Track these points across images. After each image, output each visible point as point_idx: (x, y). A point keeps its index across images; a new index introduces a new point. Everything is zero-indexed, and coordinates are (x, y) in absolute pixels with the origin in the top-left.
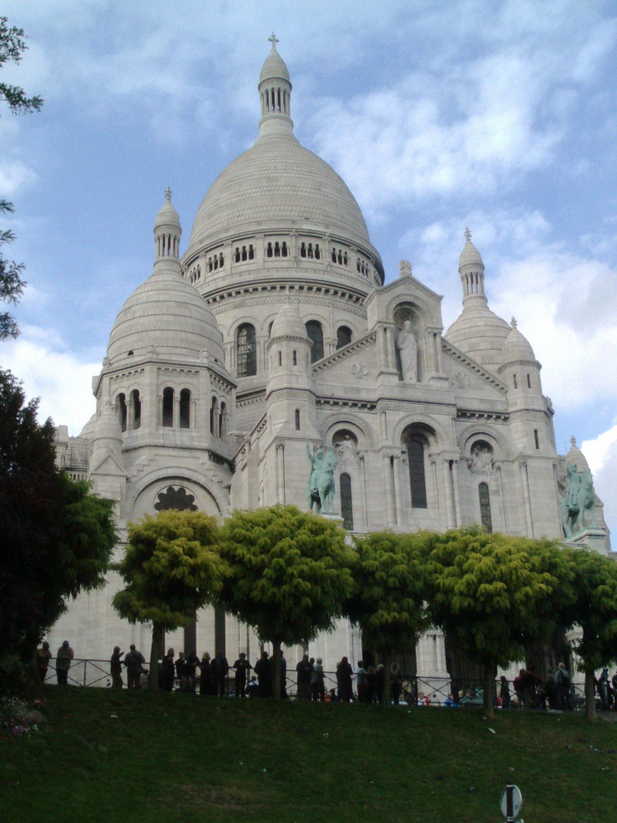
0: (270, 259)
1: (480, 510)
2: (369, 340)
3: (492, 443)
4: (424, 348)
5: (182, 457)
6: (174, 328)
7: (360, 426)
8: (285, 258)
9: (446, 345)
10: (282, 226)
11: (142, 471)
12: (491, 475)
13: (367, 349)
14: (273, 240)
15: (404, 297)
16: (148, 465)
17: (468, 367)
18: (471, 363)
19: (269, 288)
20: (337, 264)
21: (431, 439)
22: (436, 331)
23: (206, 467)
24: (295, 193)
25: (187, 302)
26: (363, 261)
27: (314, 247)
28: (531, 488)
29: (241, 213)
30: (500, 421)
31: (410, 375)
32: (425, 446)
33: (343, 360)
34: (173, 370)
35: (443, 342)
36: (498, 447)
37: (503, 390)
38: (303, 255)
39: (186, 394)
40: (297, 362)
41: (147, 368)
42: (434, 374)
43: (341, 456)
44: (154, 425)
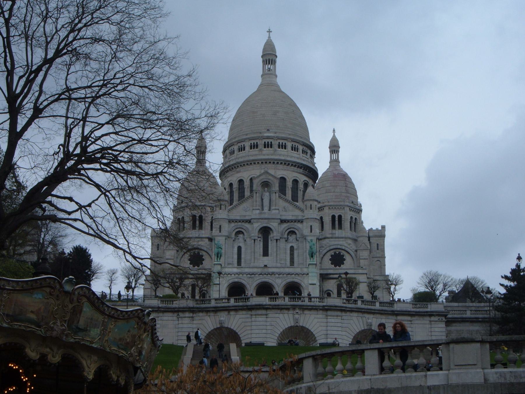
0: (251, 150)
3: (296, 231)
8: (257, 150)
10: (256, 135)
13: (250, 200)
14: (252, 142)
19: (249, 164)
20: (281, 149)
21: (271, 232)
23: (208, 244)
26: (295, 145)
27: (270, 143)
30: (299, 223)
31: (266, 209)
37: (302, 211)
38: (265, 147)
42: (274, 208)
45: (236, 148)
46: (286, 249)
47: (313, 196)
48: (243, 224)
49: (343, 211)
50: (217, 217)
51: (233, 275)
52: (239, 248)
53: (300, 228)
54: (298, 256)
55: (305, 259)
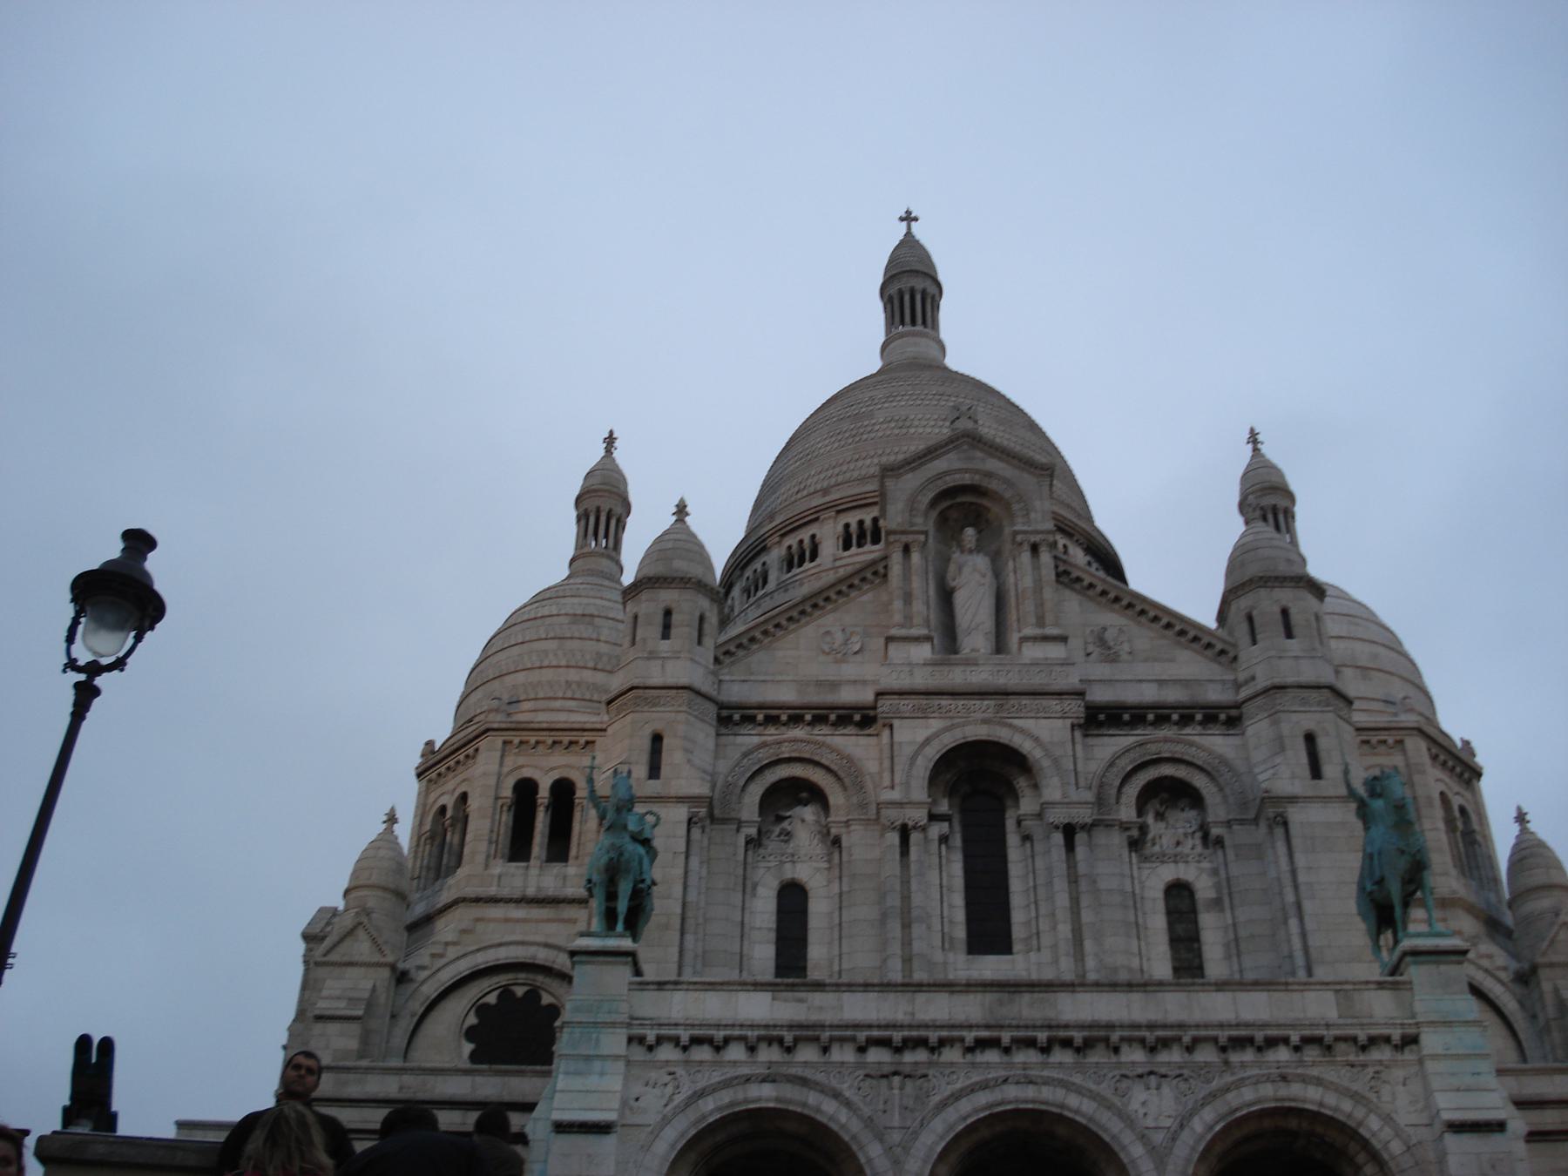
0: (847, 553)
1: (1168, 955)
2: (869, 575)
3: (1199, 781)
4: (1011, 579)
5: (538, 921)
6: (554, 663)
7: (833, 767)
9: (1069, 569)
11: (441, 956)
12: (1199, 862)
13: (865, 598)
14: (852, 519)
15: (957, 476)
16: (455, 944)
17: (1129, 612)
18: (1134, 602)
21: (1021, 783)
22: (1033, 539)
24: (904, 431)
25: (596, 613)
28: (1301, 878)
29: (802, 486)
31: (976, 641)
32: (1009, 802)
33: (802, 627)
34: (537, 742)
35: (1061, 564)
36: (1215, 790)
39: (563, 791)
40: (674, 631)
41: (483, 744)
42: (1029, 631)
43: (786, 841)
44: (481, 858)
45: (775, 556)
46: (1135, 901)
47: (1289, 561)
48: (821, 731)
49: (1397, 760)
50: (636, 682)
51: (736, 1052)
52: (793, 899)
53: (1224, 761)
54: (1234, 947)
55: (1300, 960)
